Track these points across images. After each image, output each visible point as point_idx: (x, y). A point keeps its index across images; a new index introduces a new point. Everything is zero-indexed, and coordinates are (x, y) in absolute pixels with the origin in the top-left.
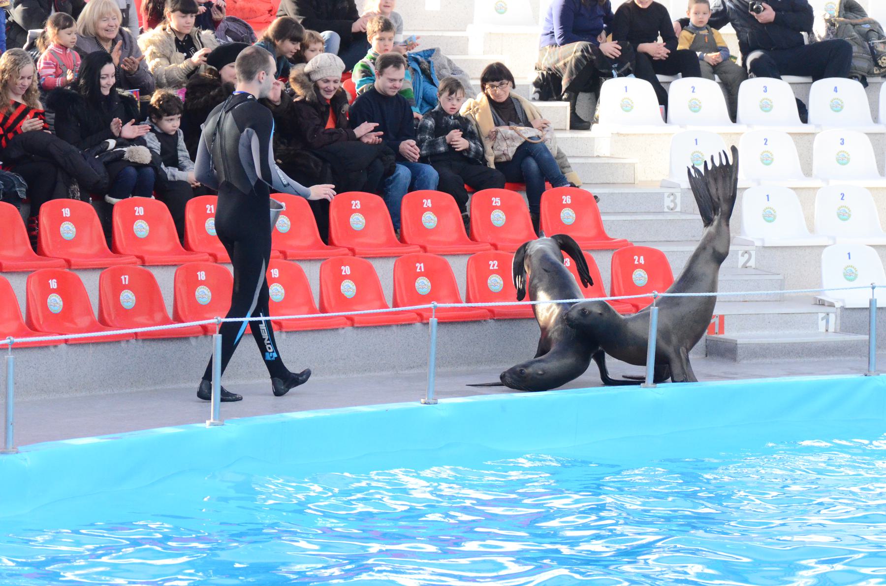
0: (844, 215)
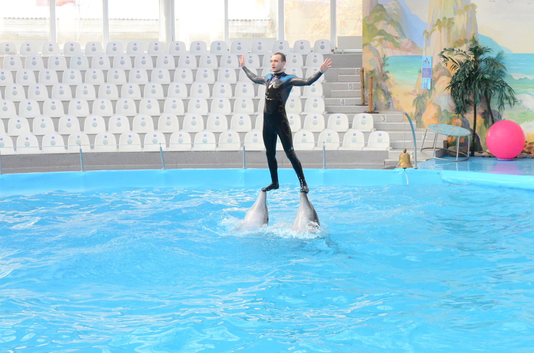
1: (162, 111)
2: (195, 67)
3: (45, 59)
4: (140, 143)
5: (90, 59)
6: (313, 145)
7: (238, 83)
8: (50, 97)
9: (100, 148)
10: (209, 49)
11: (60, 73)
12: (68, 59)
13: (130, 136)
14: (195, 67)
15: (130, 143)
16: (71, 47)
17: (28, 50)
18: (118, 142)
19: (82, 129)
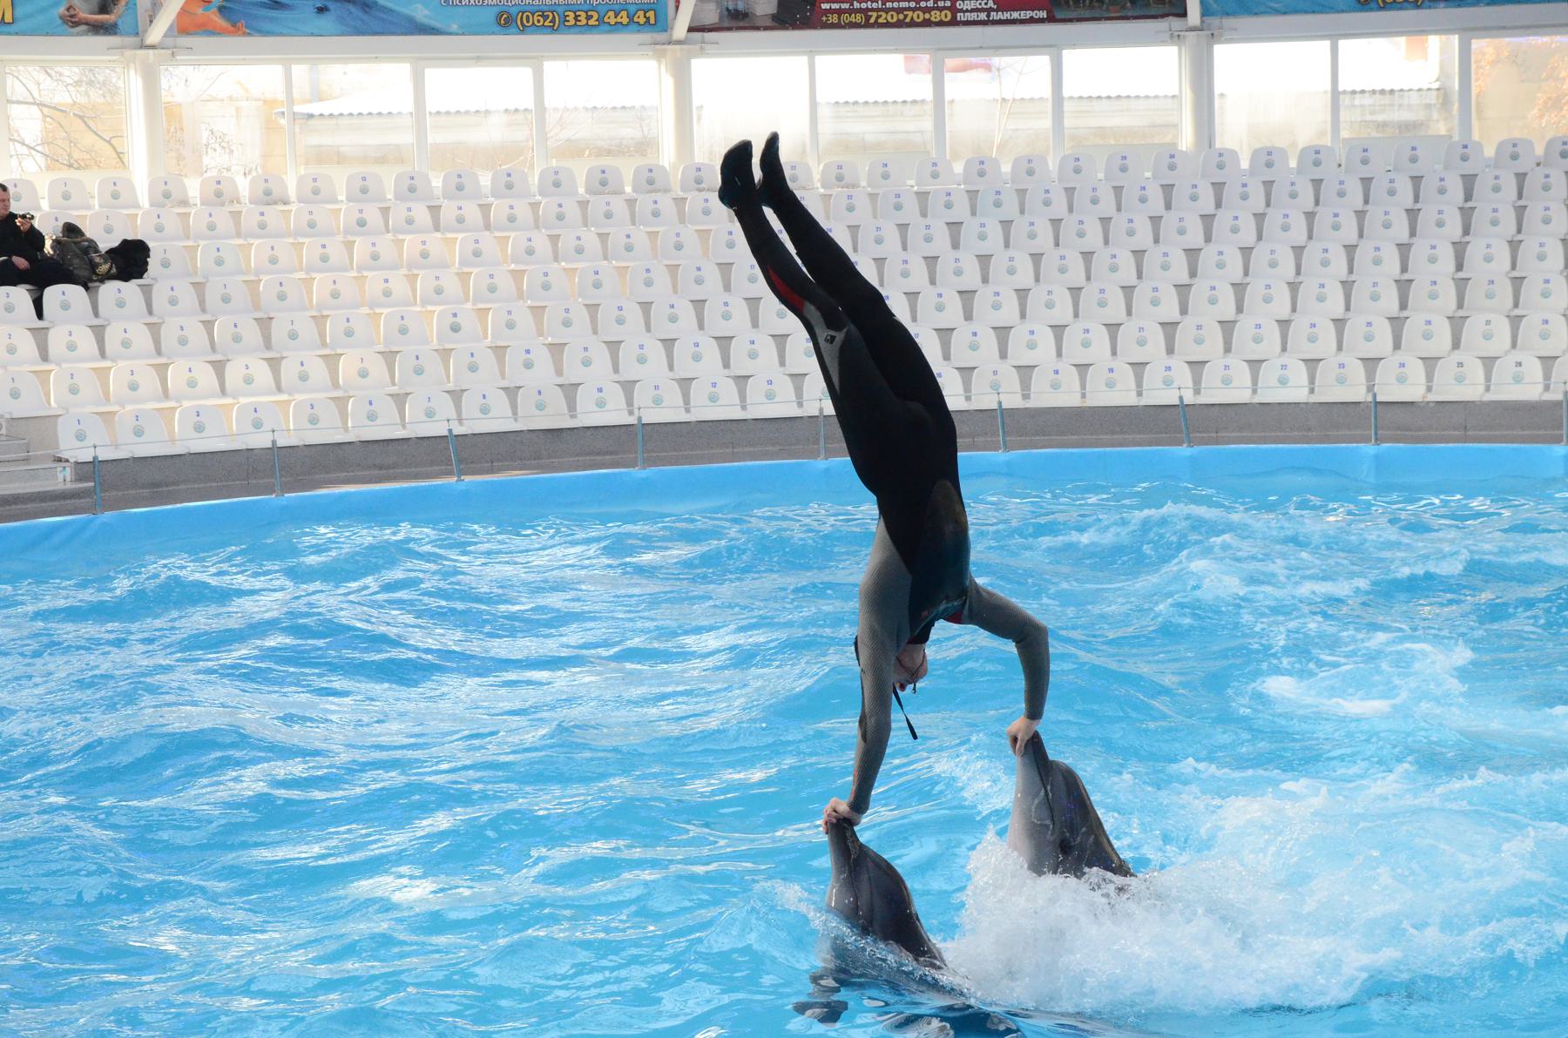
0: (74, 390)
1: (1184, 310)
2: (1260, 206)
3: (922, 196)
4: (1133, 385)
5: (1022, 193)
6: (1540, 387)
7: (1362, 243)
8: (933, 282)
9: (1044, 397)
10: (1293, 164)
11: (954, 227)
12: (973, 194)
13: (1111, 370)
14: (1260, 206)
15: (1110, 385)
16: (981, 167)
17: (886, 176)
18: (1083, 386)
19: (1003, 355)
